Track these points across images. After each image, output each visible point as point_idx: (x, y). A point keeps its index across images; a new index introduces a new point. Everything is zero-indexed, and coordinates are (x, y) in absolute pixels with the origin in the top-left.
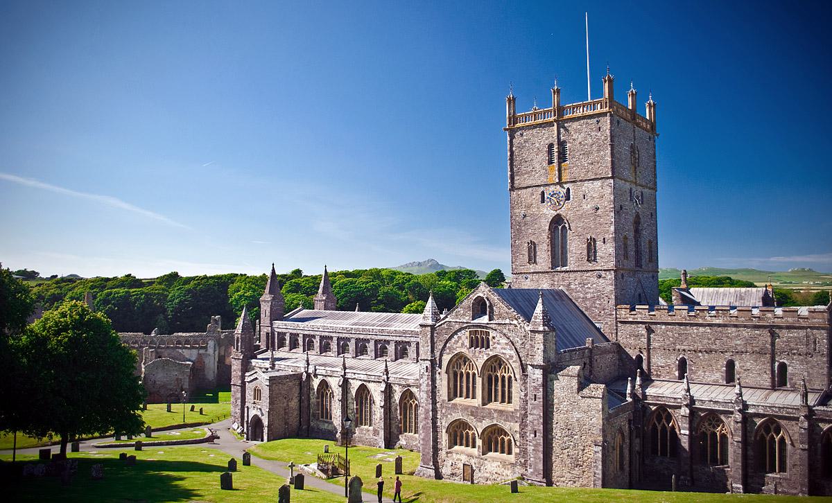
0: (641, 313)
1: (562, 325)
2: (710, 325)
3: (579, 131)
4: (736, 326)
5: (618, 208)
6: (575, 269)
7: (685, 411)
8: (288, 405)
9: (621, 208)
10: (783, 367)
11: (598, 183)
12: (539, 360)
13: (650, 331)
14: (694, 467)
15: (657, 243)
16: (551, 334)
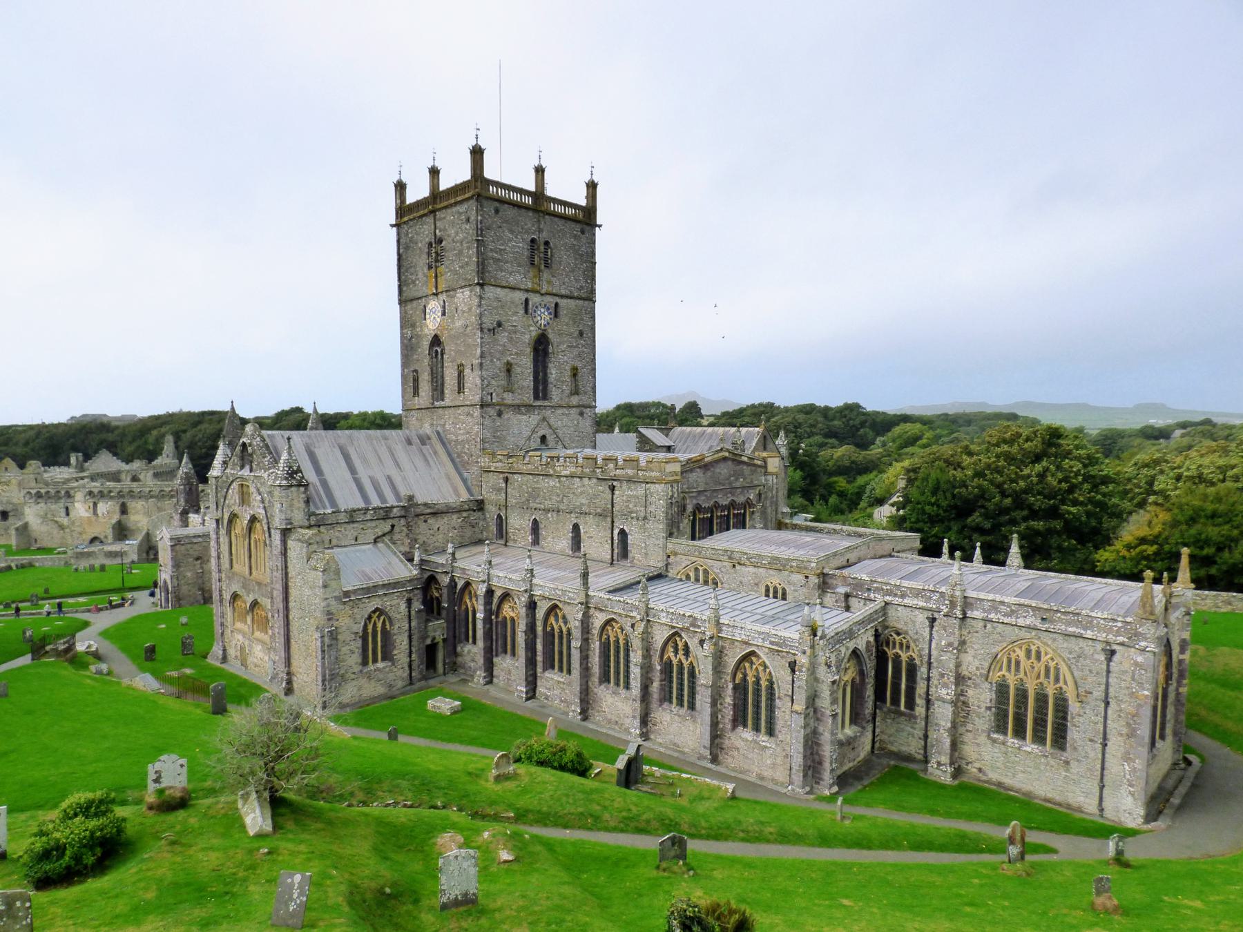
0: (501, 461)
1: (389, 478)
2: (559, 477)
3: (453, 224)
4: (580, 478)
5: (489, 322)
6: (450, 404)
7: (481, 589)
8: (202, 568)
9: (499, 324)
10: (623, 533)
11: (467, 292)
12: (278, 522)
13: (506, 480)
14: (495, 660)
15: (594, 369)
16: (293, 489)
